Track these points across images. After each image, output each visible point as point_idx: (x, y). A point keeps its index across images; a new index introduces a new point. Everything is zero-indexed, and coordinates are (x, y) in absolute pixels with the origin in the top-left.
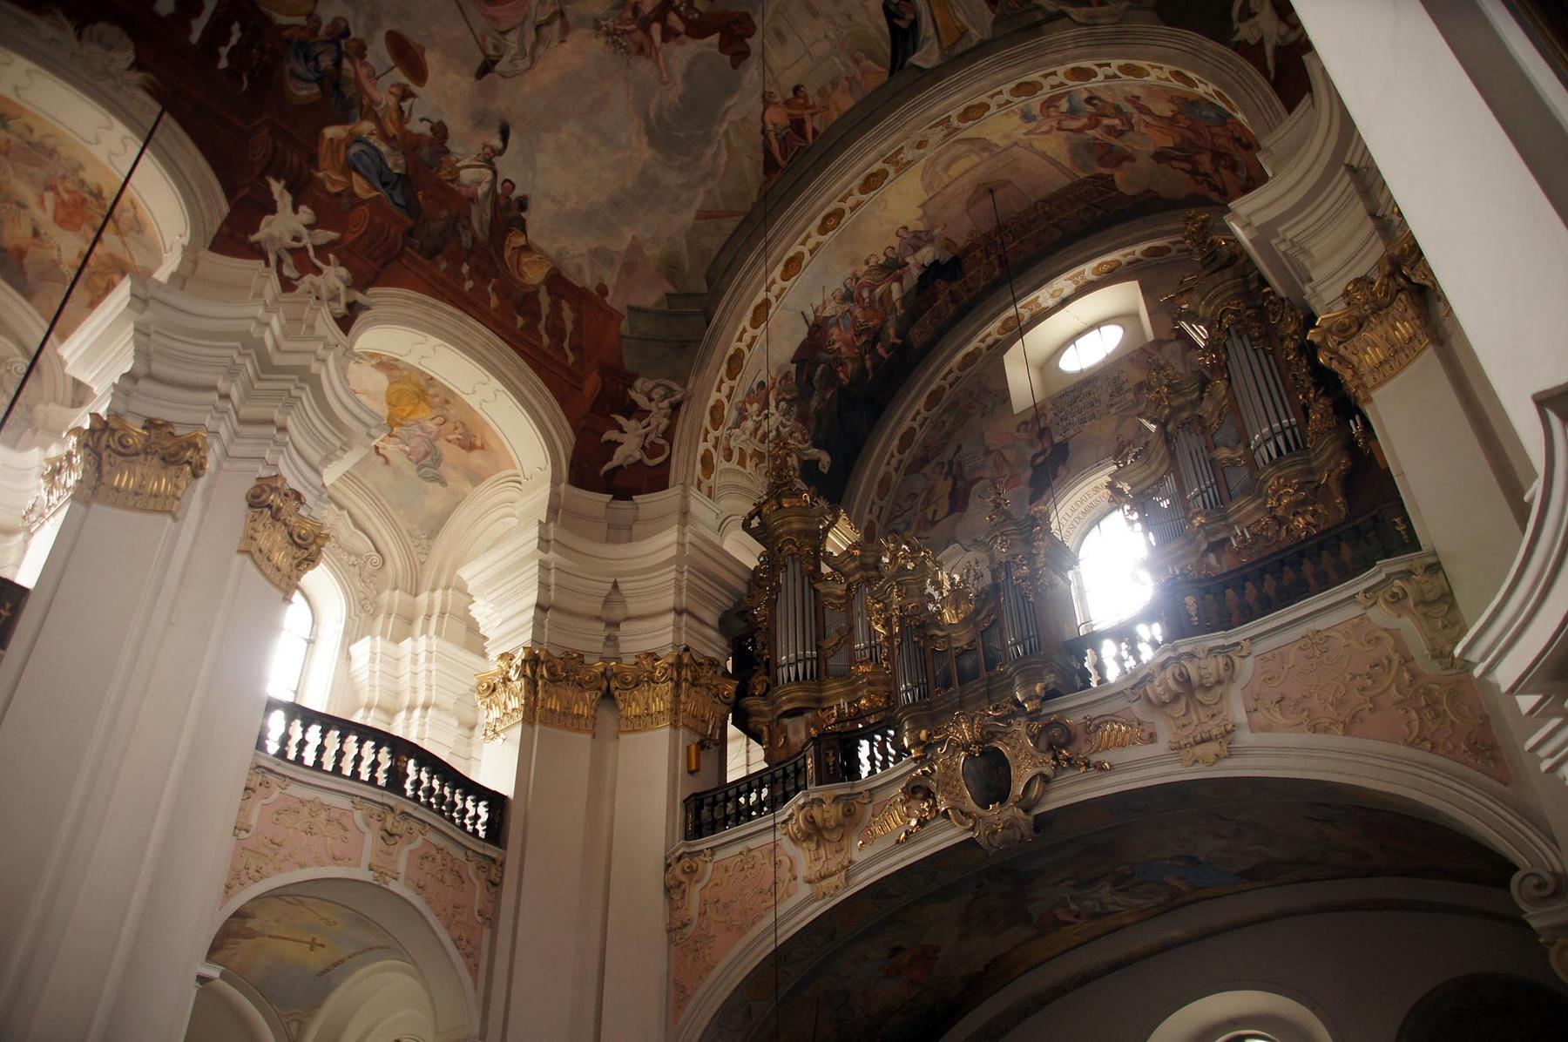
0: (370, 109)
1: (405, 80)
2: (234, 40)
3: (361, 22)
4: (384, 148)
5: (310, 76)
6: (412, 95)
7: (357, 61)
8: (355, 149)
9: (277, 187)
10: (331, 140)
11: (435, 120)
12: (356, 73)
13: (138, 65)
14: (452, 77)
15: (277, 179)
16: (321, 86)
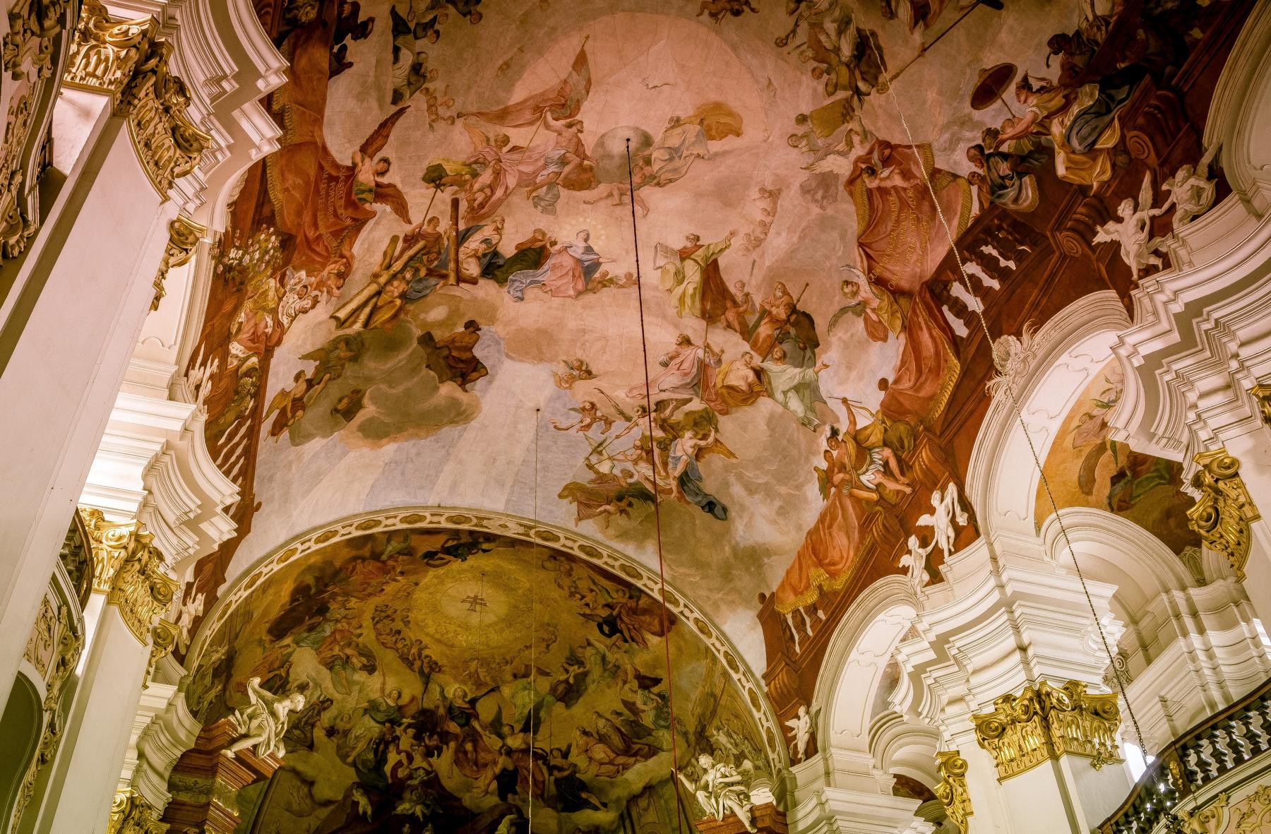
0: (1041, 124)
1: (1013, 87)
2: (995, 253)
3: (968, 134)
4: (1075, 109)
5: (1017, 183)
6: (1025, 79)
7: (1000, 137)
8: (1075, 143)
9: (1102, 237)
10: (1067, 168)
11: (1048, 50)
12: (1011, 138)
13: (1018, 335)
14: (1004, 36)
15: (1095, 234)
16: (1026, 174)
